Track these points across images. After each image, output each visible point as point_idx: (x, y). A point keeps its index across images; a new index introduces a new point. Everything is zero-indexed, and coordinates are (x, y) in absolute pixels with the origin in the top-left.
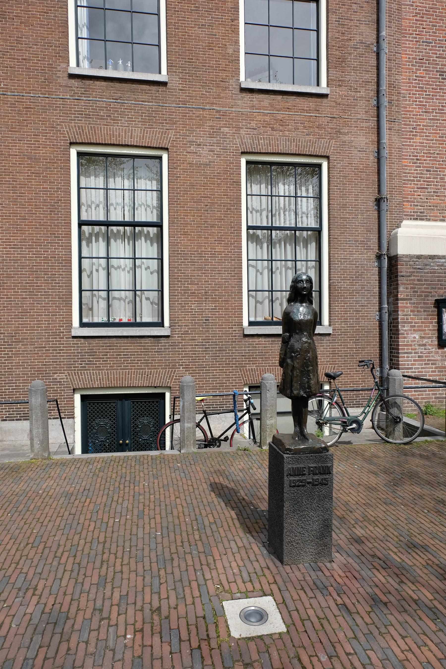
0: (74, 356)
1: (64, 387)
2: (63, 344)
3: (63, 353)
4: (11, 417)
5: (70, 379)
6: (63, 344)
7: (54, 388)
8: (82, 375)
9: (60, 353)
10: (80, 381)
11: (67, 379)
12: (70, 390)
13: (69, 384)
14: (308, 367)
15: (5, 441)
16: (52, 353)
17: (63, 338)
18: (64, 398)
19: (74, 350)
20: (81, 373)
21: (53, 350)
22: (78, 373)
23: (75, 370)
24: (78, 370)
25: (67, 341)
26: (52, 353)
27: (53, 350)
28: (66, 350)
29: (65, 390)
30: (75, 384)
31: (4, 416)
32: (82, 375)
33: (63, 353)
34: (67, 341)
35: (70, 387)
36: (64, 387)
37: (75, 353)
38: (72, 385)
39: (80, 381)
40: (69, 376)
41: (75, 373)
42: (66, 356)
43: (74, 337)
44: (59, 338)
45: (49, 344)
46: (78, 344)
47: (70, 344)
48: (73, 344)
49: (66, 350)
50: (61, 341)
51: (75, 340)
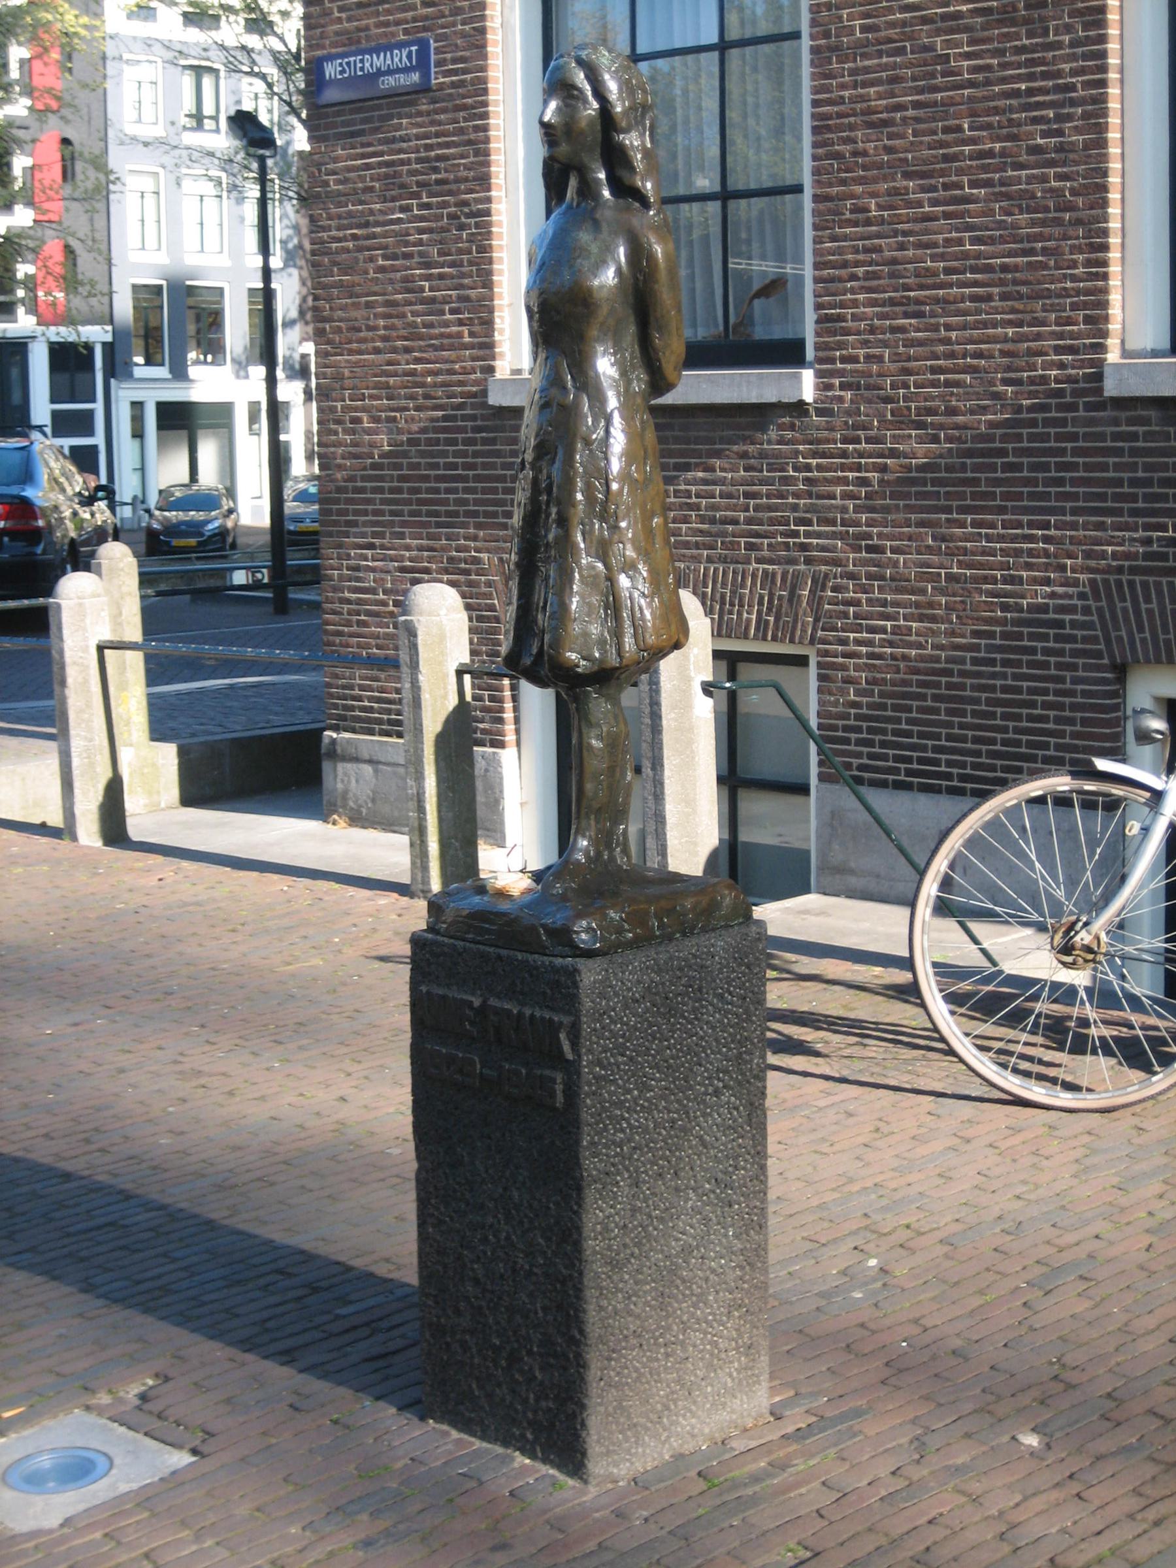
0: (1118, 497)
1: (1075, 653)
2: (1074, 437)
3: (1075, 482)
4: (877, 770)
5: (1100, 611)
6: (1074, 437)
7: (1033, 651)
8: (1148, 600)
9: (1060, 482)
10: (1141, 629)
11: (1086, 610)
12: (1099, 668)
13: (1095, 640)
14: (548, 530)
15: (852, 872)
16: (1027, 482)
17: (1072, 407)
18: (1074, 707)
19: (1118, 467)
20: (1145, 585)
21: (1034, 467)
22: (1131, 584)
23: (1120, 570)
24: (1133, 570)
25: (1091, 422)
26: (1027, 482)
27: (1034, 467)
28: (1088, 467)
29: (1073, 667)
30: (1120, 639)
31: (855, 762)
32: (1148, 600)
33: (1075, 482)
34: (1091, 422)
35: (1098, 655)
36: (1075, 653)
37: (1119, 483)
38: (1108, 641)
39: (1141, 629)
40: (1097, 598)
41: (1119, 584)
42: (1089, 497)
43: (1120, 403)
44: (1061, 407)
45: (1019, 438)
46: (1134, 437)
47: (1101, 437)
48: (1117, 437)
49: (1088, 467)
50: (1063, 422)
51: (1124, 415)
